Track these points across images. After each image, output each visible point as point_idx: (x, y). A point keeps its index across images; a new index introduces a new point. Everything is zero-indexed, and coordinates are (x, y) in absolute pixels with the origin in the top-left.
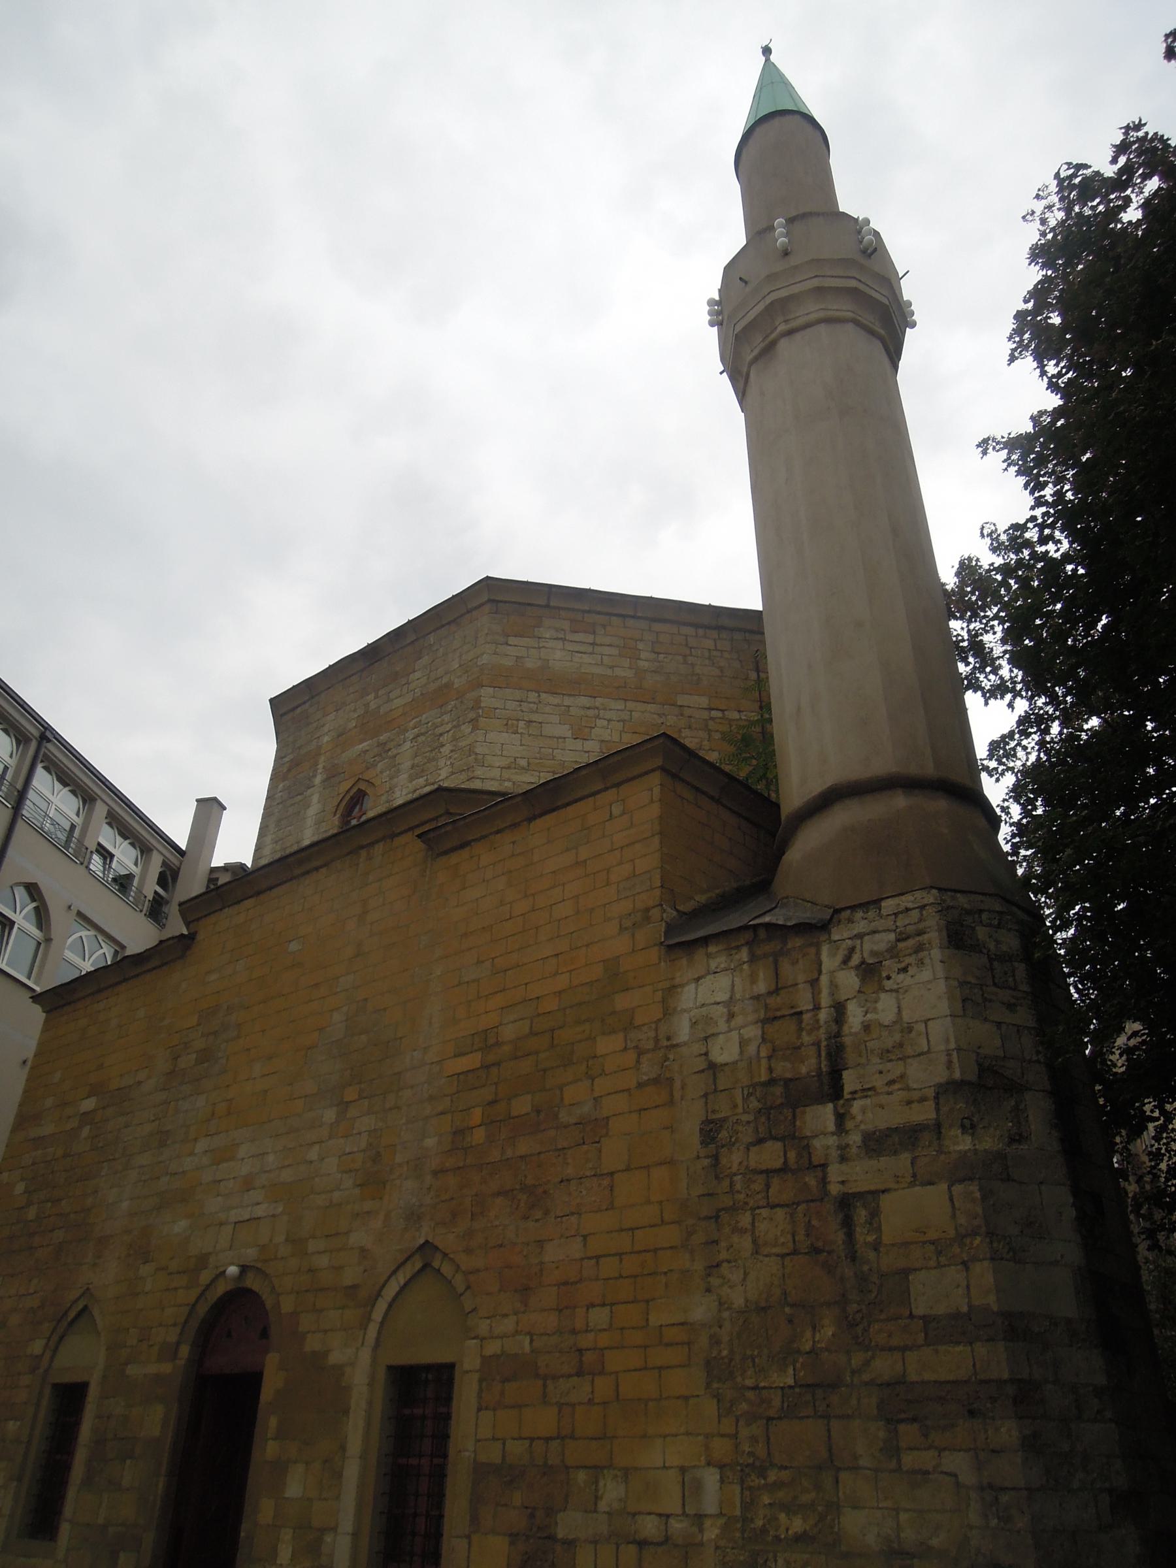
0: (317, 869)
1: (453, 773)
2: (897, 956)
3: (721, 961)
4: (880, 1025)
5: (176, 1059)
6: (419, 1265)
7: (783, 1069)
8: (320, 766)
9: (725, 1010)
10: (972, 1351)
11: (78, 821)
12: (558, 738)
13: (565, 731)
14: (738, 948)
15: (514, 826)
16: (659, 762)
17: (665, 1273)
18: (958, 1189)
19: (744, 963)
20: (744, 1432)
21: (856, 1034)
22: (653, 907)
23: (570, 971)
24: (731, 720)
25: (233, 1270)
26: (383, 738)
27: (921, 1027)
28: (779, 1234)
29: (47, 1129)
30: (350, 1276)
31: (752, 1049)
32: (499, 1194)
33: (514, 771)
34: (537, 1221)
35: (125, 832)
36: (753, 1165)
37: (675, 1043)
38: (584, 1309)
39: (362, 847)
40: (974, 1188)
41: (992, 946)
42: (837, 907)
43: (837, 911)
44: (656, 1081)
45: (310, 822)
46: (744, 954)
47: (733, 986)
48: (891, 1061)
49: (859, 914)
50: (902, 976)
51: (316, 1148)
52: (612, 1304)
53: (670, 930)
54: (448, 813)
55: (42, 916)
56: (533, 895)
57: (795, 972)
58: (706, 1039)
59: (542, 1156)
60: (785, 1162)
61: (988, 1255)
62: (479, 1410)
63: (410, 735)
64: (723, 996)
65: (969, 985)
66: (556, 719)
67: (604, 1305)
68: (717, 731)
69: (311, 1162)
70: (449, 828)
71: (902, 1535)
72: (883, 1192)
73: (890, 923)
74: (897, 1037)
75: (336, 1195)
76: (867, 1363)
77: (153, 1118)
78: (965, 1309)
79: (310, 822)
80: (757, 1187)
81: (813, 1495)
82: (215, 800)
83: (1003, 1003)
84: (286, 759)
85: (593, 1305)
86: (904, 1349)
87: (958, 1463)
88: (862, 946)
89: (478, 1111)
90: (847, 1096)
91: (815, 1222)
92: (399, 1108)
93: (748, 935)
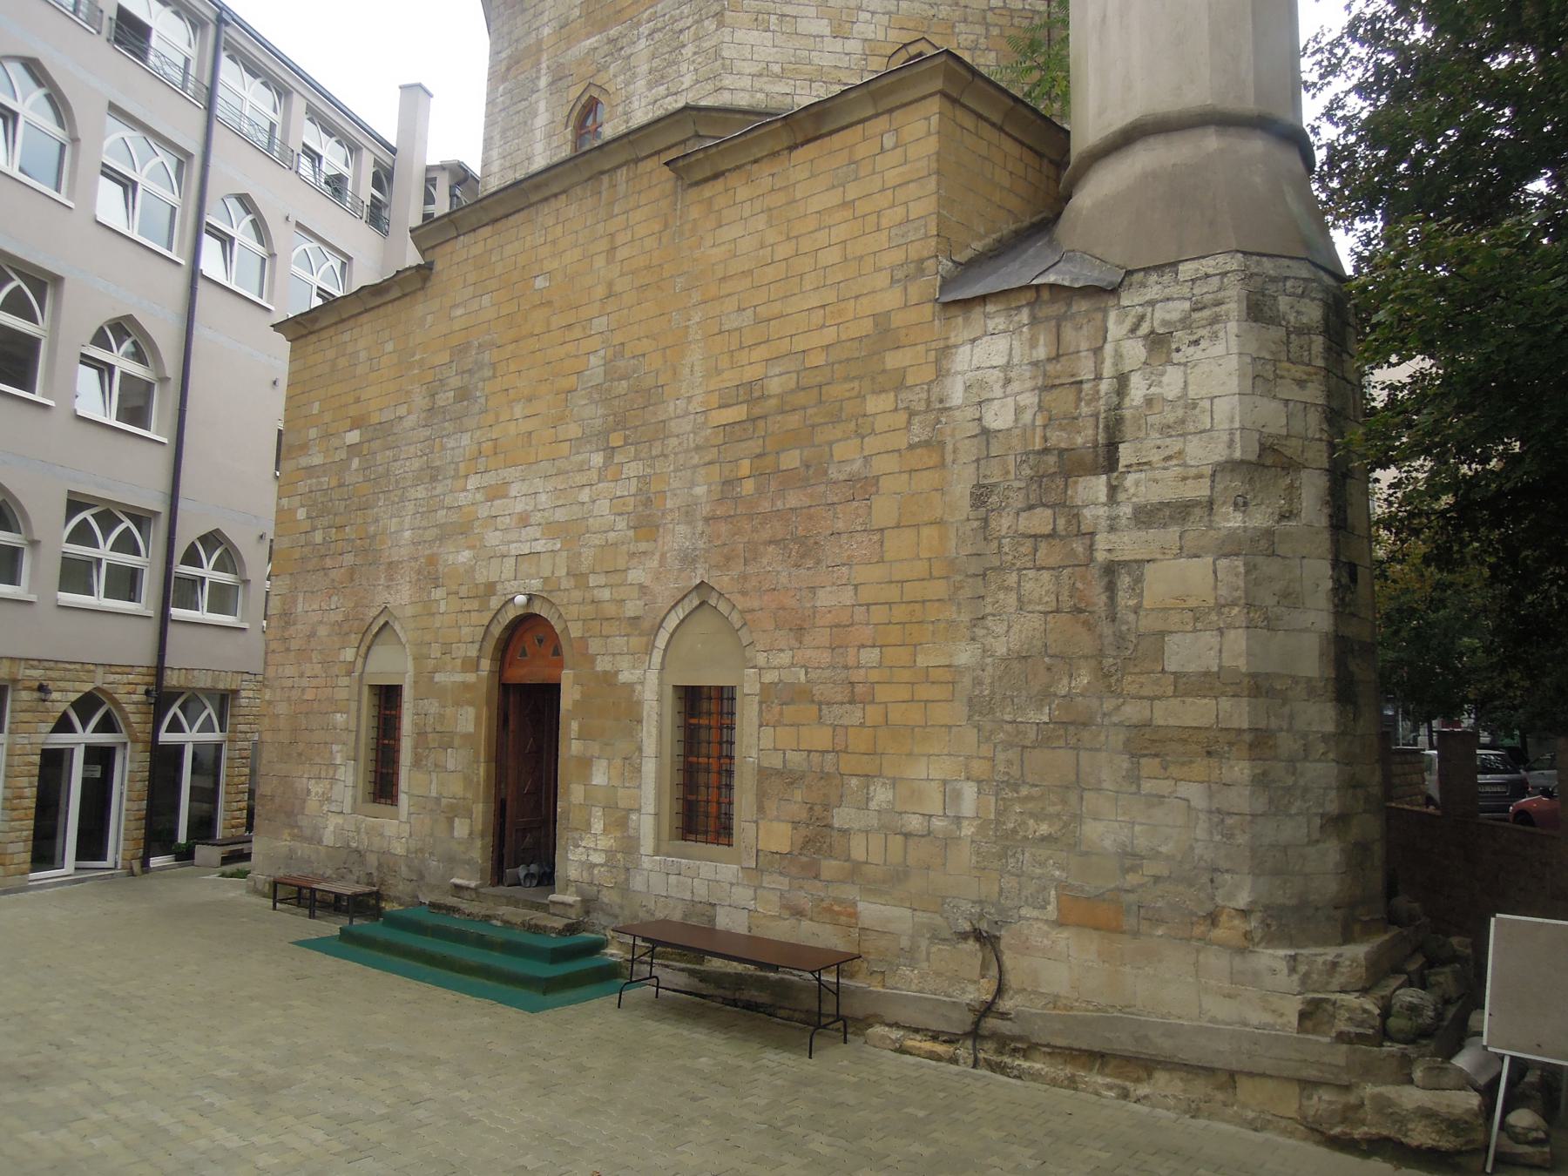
0: (556, 195)
1: (697, 82)
2: (1190, 327)
3: (998, 322)
4: (1164, 399)
5: (433, 395)
6: (696, 602)
7: (1058, 438)
8: (544, 66)
9: (1002, 375)
10: (1217, 704)
11: (277, 118)
12: (814, 37)
13: (823, 27)
14: (1019, 308)
15: (774, 154)
16: (938, 84)
17: (933, 622)
18: (1223, 563)
19: (1024, 325)
20: (1001, 756)
21: (1136, 408)
22: (929, 258)
23: (839, 324)
24: (1012, 10)
25: (521, 599)
26: (613, 32)
27: (1206, 404)
28: (1043, 593)
29: (317, 460)
30: (632, 608)
31: (1027, 417)
32: (770, 542)
33: (766, 79)
34: (809, 569)
35: (329, 129)
36: (1021, 529)
37: (947, 405)
38: (856, 649)
39: (602, 173)
40: (1239, 563)
41: (1292, 319)
42: (1130, 268)
43: (1129, 273)
44: (926, 444)
45: (539, 134)
46: (1024, 316)
47: (1011, 349)
48: (1171, 436)
49: (1154, 277)
50: (1192, 349)
51: (587, 490)
52: (881, 646)
53: (946, 284)
54: (698, 136)
55: (260, 229)
56: (797, 237)
57: (1078, 338)
58: (980, 403)
59: (812, 510)
60: (1054, 529)
61: (1244, 625)
62: (760, 726)
63: (645, 29)
64: (1002, 361)
65: (1262, 361)
66: (812, 11)
67: (874, 646)
68: (996, 25)
69: (584, 503)
70: (701, 155)
71: (1135, 842)
72: (1148, 561)
73: (1186, 290)
74: (1180, 413)
75: (612, 535)
76: (1118, 708)
77: (419, 453)
78: (1215, 669)
79: (539, 134)
80: (1023, 550)
81: (1059, 808)
82: (420, 86)
83: (1293, 380)
84: (504, 55)
85: (863, 646)
86: (1152, 699)
87: (1194, 792)
88: (1152, 314)
89: (746, 463)
90: (1121, 469)
91: (1079, 585)
92: (666, 456)
93: (1031, 295)
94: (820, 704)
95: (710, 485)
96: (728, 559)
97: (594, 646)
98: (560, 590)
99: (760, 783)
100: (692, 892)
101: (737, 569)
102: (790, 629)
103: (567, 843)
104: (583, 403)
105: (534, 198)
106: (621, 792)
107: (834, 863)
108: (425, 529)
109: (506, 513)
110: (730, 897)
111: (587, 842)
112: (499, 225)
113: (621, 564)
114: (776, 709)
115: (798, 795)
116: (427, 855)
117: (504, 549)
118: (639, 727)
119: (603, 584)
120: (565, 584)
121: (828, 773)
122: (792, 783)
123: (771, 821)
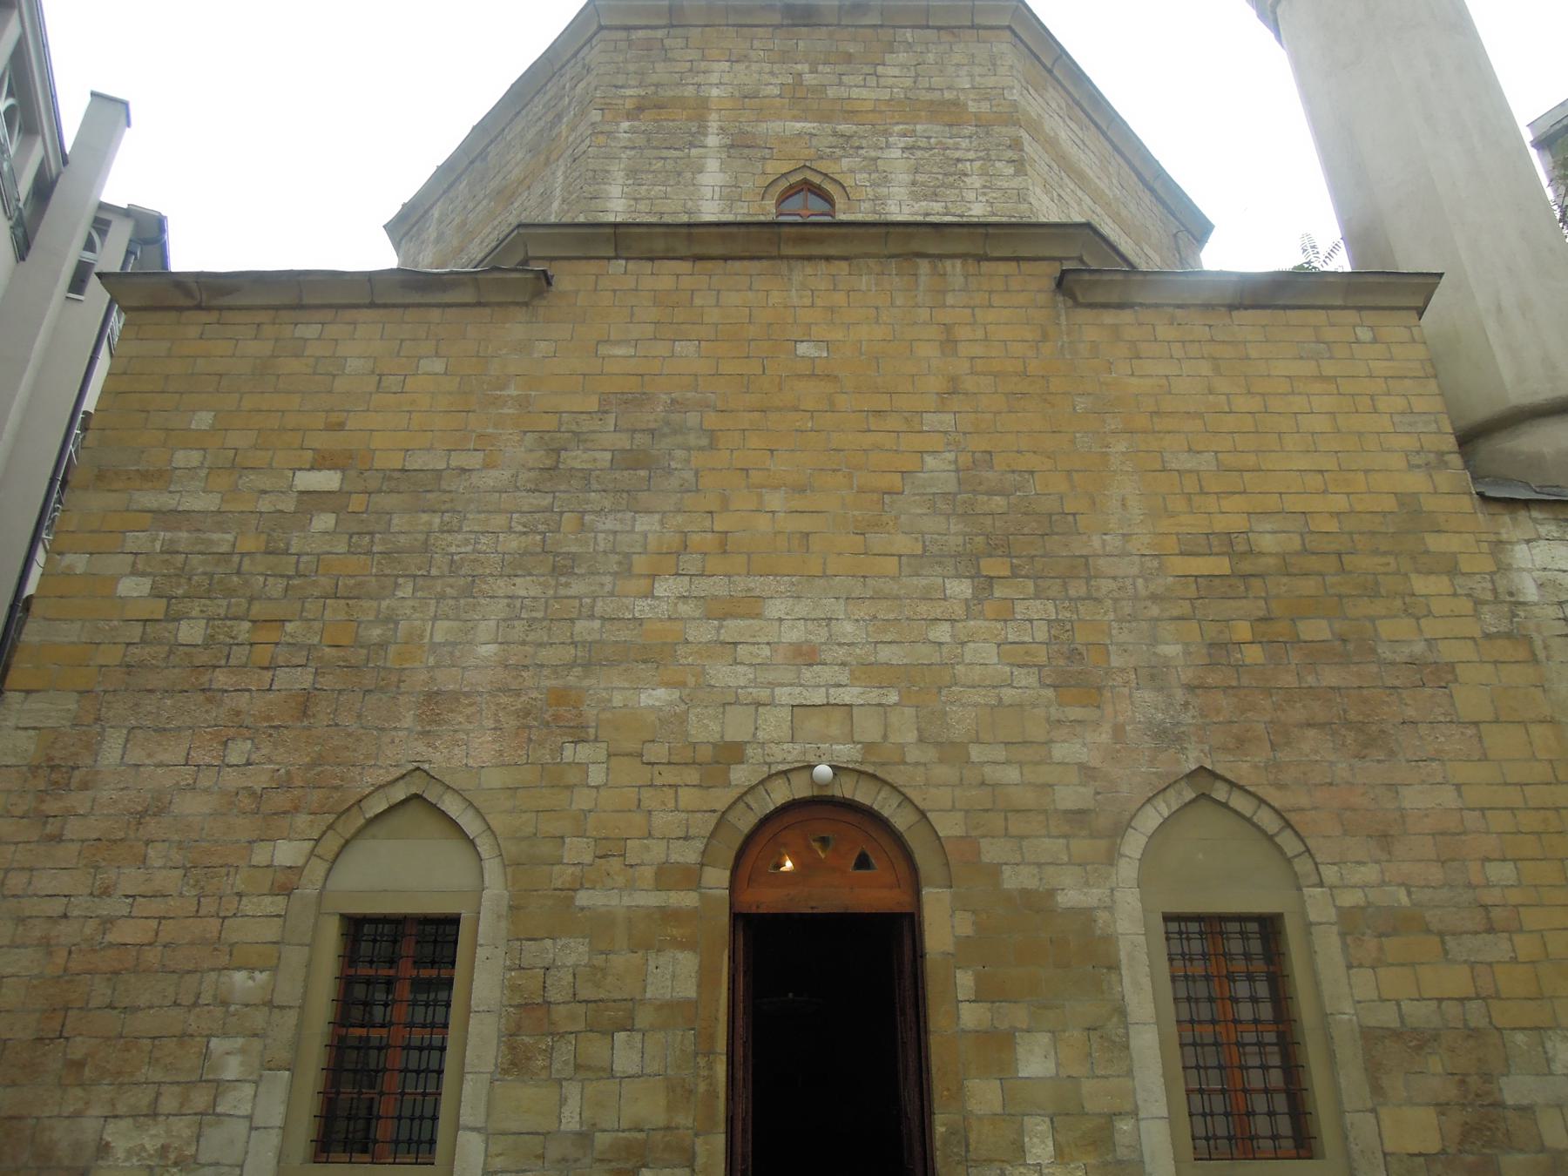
6: (1189, 795)
30: (1070, 796)
32: (1309, 725)
37: (1521, 600)
69: (940, 644)
94: (1441, 934)
95: (1187, 644)
97: (992, 852)
102: (1369, 836)
104: (919, 511)
105: (787, 250)
106: (1087, 1086)
107: (1520, 1157)
108: (541, 645)
112: (699, 265)
115: (1435, 1064)
117: (763, 694)
118: (1114, 977)
119: (1002, 758)
120: (913, 755)
121: (1476, 1030)
122: (1420, 1048)
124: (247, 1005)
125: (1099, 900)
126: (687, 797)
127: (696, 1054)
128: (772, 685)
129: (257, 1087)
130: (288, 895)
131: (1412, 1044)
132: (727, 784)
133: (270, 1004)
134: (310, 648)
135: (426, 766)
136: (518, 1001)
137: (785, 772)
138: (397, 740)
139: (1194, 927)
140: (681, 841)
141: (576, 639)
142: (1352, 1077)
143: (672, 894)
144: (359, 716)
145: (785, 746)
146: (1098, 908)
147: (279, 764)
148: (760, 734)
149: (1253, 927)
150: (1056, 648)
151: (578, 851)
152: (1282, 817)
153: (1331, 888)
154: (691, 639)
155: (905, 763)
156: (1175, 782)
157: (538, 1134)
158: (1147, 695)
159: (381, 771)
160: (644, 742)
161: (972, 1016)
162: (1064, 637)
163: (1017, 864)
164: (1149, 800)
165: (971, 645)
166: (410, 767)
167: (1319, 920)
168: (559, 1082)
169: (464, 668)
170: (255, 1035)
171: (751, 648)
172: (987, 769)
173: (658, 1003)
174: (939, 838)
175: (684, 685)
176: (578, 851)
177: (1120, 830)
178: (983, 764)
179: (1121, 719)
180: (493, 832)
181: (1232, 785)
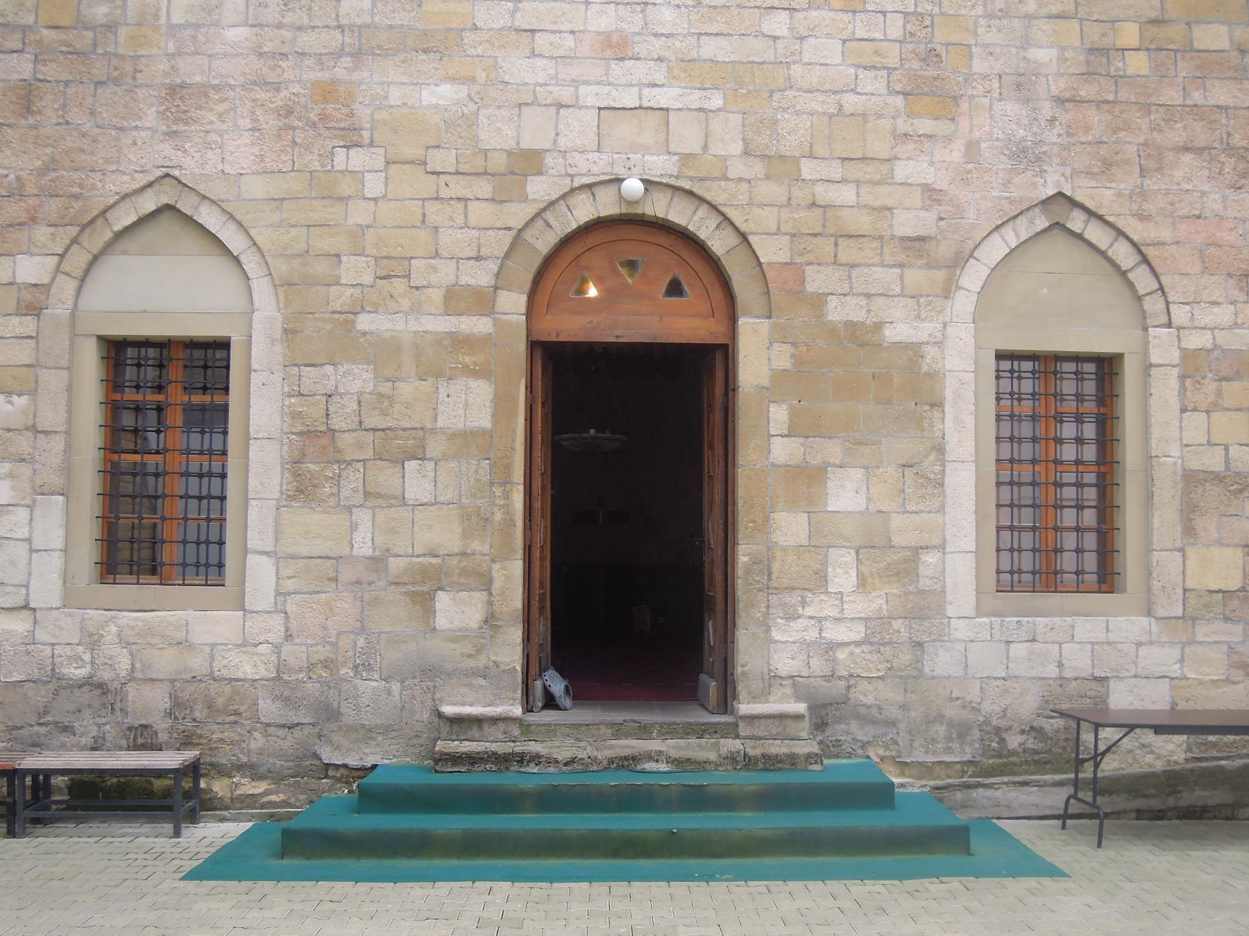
6: (1043, 223)
30: (907, 223)
32: (1187, 149)
69: (775, 38)
95: (1063, 49)
96: (1108, 165)
97: (817, 280)
98: (725, 178)
99: (1186, 493)
100: (1060, 665)
101: (1127, 180)
102: (1230, 275)
103: (766, 615)
106: (896, 521)
109: (566, 27)
110: (1136, 664)
111: (820, 606)
113: (879, 148)
114: (1210, 387)
116: (346, 671)
117: (565, 94)
119: (838, 177)
120: (737, 169)
122: (1241, 491)
123: (1208, 546)
124: (9, 430)
125: (930, 335)
126: (480, 213)
127: (492, 484)
128: (576, 83)
129: (32, 511)
130: (38, 315)
131: (1232, 488)
132: (524, 198)
133: (34, 429)
134: (25, 29)
135: (176, 173)
136: (299, 428)
137: (590, 186)
138: (139, 142)
139: (1027, 366)
140: (472, 262)
141: (343, 22)
142: (1166, 520)
143: (463, 318)
144: (93, 113)
145: (590, 156)
146: (927, 343)
147: (7, 168)
148: (563, 142)
149: (1090, 367)
150: (910, 47)
151: (356, 270)
152: (1140, 252)
153: (1179, 329)
154: (479, 24)
155: (727, 179)
156: (1028, 209)
157: (328, 558)
158: (1010, 108)
159: (126, 178)
160: (428, 148)
161: (783, 450)
162: (921, 34)
163: (845, 295)
164: (998, 228)
165: (812, 41)
166: (159, 173)
167: (1160, 362)
168: (349, 509)
169: (210, 56)
170: (23, 460)
171: (551, 37)
172: (820, 189)
173: (451, 432)
174: (760, 264)
175: (473, 80)
176: (356, 270)
177: (960, 260)
178: (815, 182)
179: (976, 135)
180: (259, 249)
181: (1091, 214)
